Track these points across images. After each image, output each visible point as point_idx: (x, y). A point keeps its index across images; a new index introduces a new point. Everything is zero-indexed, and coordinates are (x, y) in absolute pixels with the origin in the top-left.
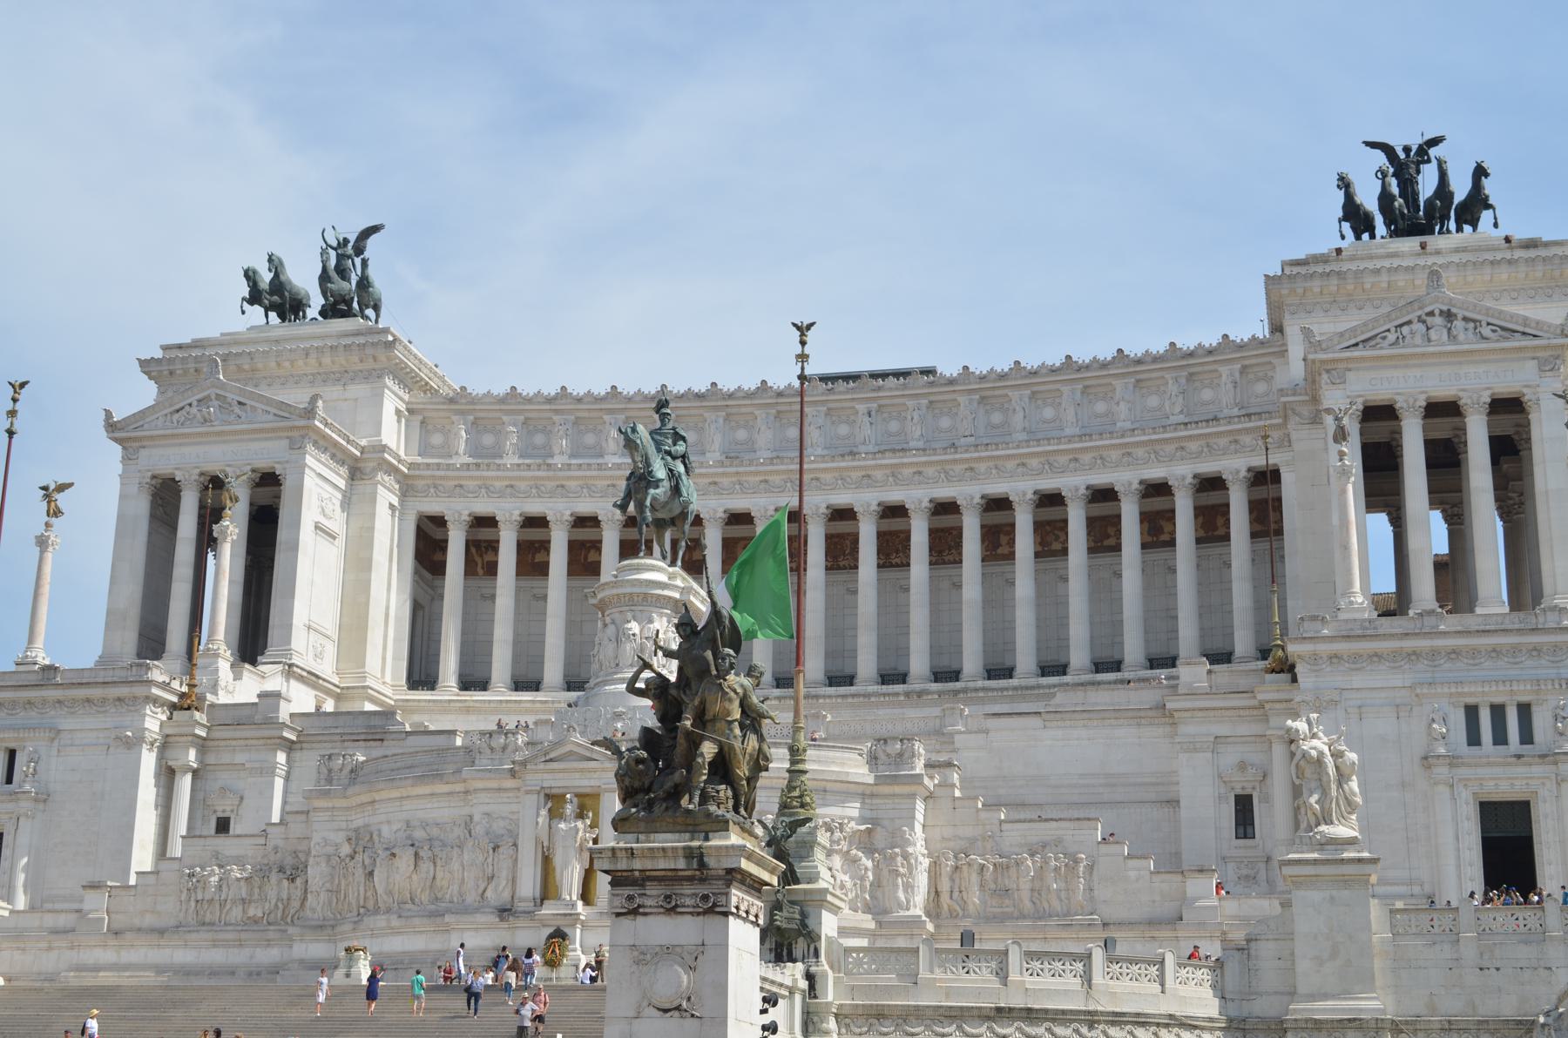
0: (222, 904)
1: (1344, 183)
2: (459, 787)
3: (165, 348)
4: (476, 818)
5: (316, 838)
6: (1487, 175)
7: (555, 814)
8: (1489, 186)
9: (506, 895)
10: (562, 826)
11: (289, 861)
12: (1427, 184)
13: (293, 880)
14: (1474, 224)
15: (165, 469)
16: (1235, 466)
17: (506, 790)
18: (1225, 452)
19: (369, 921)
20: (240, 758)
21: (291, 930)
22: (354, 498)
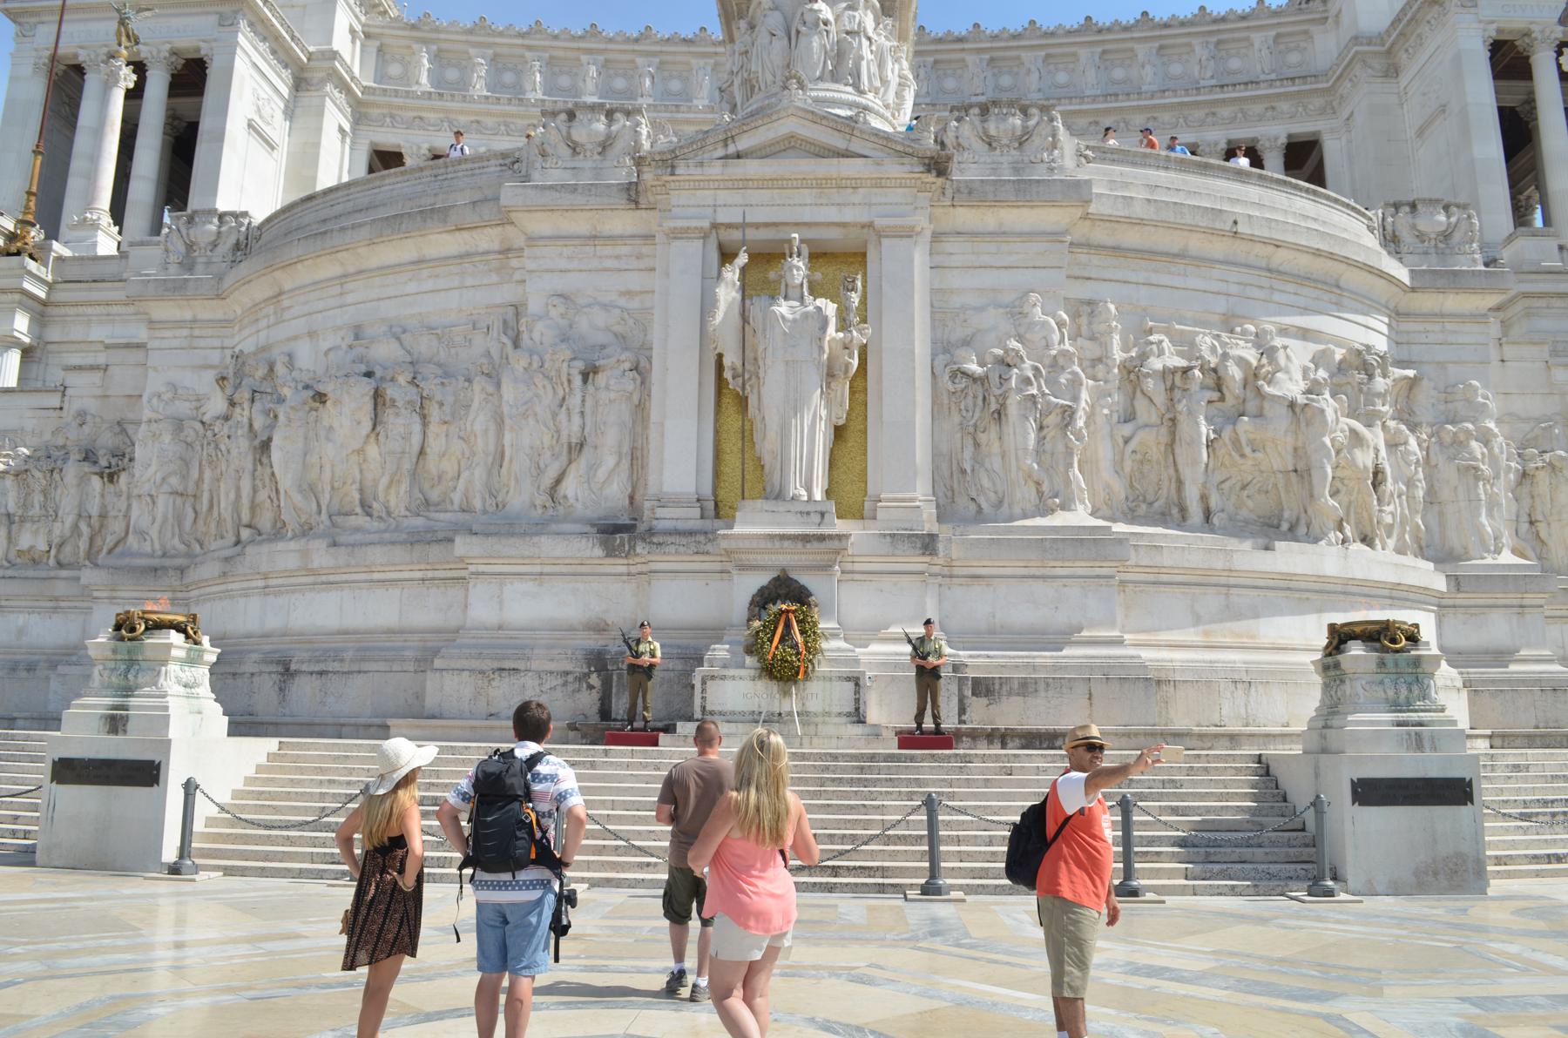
2: (487, 239)
4: (534, 306)
10: (783, 308)
11: (107, 440)
13: (112, 478)
17: (611, 239)
18: (1261, 118)
19: (259, 556)
21: (88, 576)
22: (298, 111)
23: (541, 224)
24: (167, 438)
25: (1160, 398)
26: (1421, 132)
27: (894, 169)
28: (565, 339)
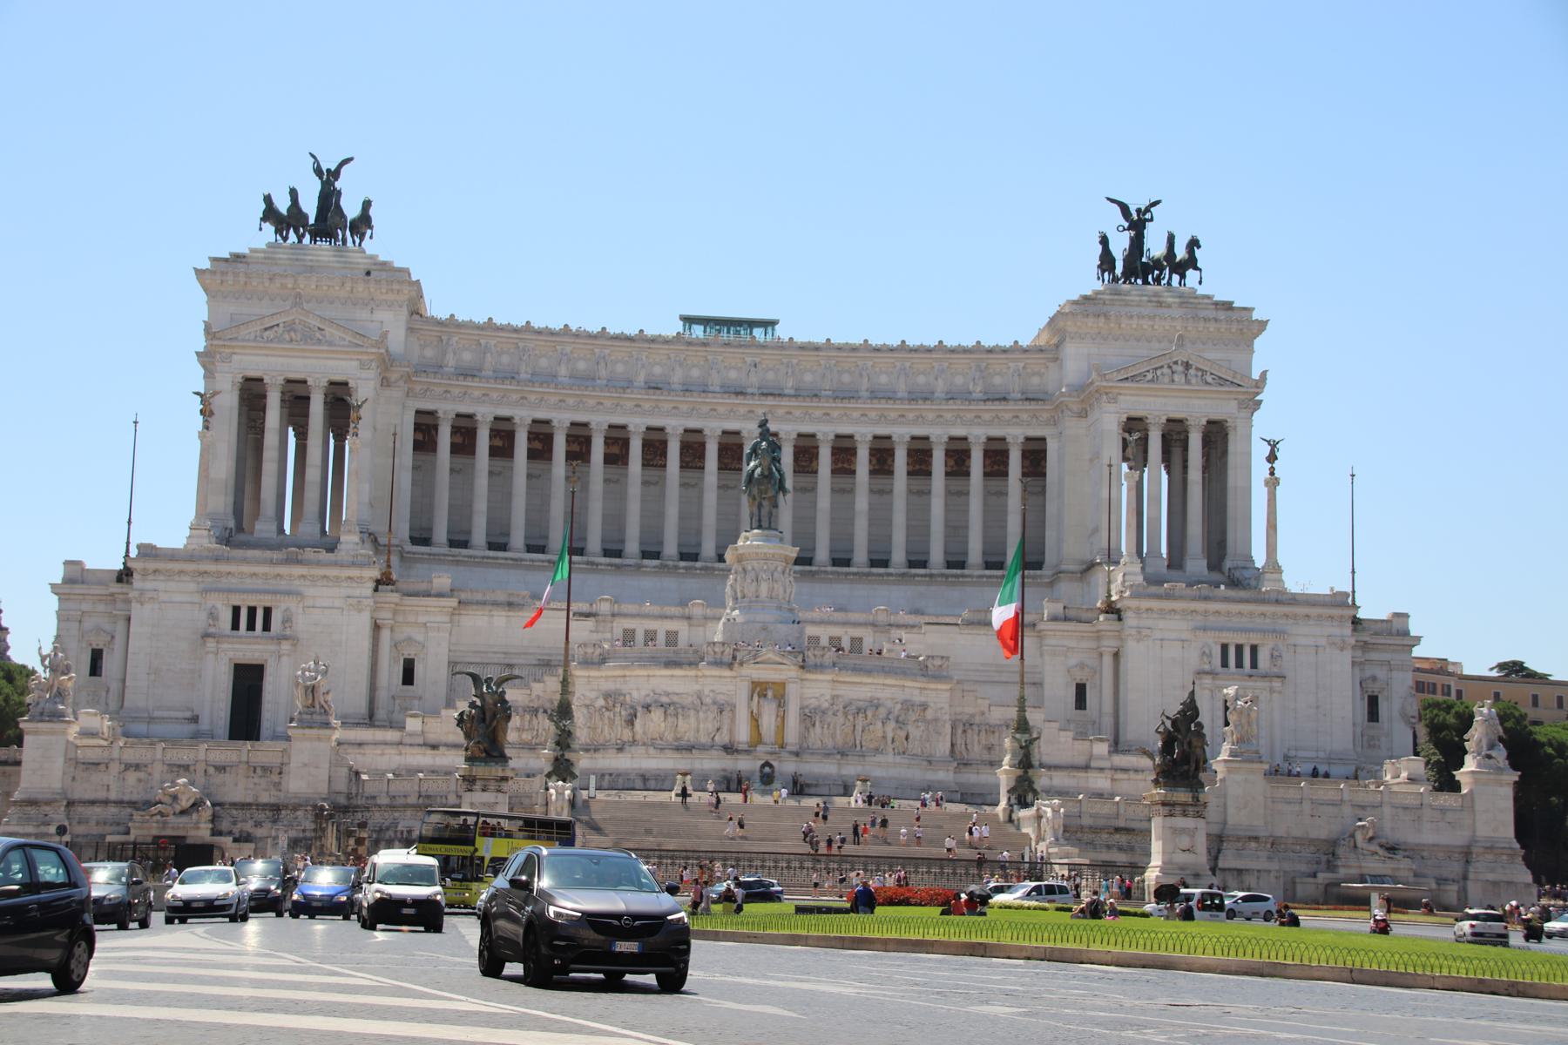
1: (1104, 241)
2: (692, 673)
3: (214, 260)
7: (763, 695)
8: (1198, 253)
9: (726, 740)
12: (1155, 246)
14: (1183, 276)
16: (1015, 435)
20: (422, 619)
23: (707, 673)
26: (1091, 461)
28: (715, 703)
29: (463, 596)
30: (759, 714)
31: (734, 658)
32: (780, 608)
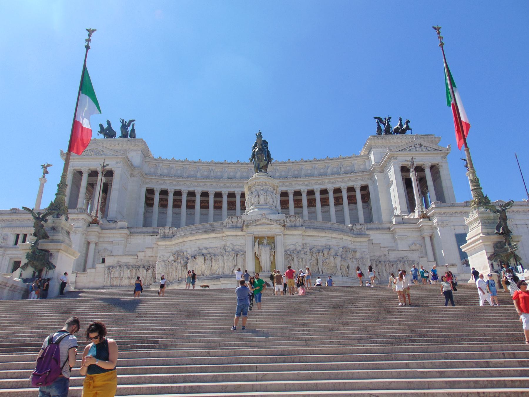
0: (121, 279)
2: (220, 235)
4: (228, 245)
5: (159, 255)
6: (409, 122)
7: (260, 243)
11: (146, 264)
13: (147, 270)
15: (78, 168)
16: (357, 185)
20: (111, 240)
23: (228, 233)
24: (163, 264)
25: (315, 257)
27: (278, 226)
28: (233, 250)
29: (132, 230)
30: (260, 255)
31: (244, 224)
32: (271, 208)
